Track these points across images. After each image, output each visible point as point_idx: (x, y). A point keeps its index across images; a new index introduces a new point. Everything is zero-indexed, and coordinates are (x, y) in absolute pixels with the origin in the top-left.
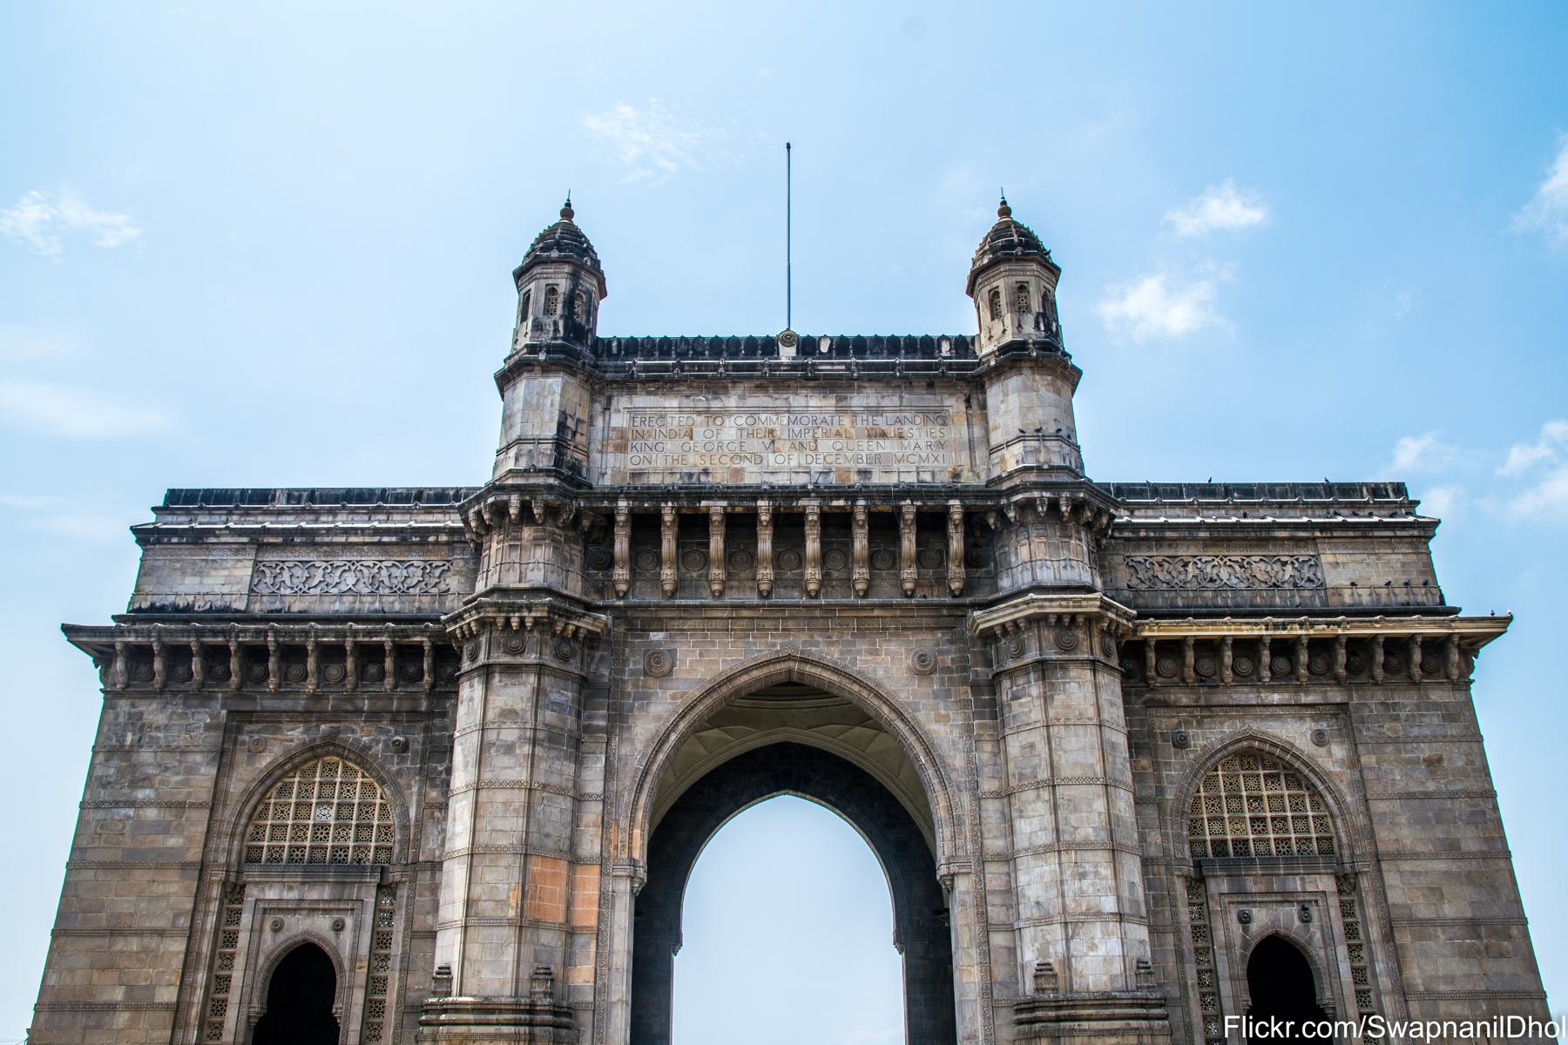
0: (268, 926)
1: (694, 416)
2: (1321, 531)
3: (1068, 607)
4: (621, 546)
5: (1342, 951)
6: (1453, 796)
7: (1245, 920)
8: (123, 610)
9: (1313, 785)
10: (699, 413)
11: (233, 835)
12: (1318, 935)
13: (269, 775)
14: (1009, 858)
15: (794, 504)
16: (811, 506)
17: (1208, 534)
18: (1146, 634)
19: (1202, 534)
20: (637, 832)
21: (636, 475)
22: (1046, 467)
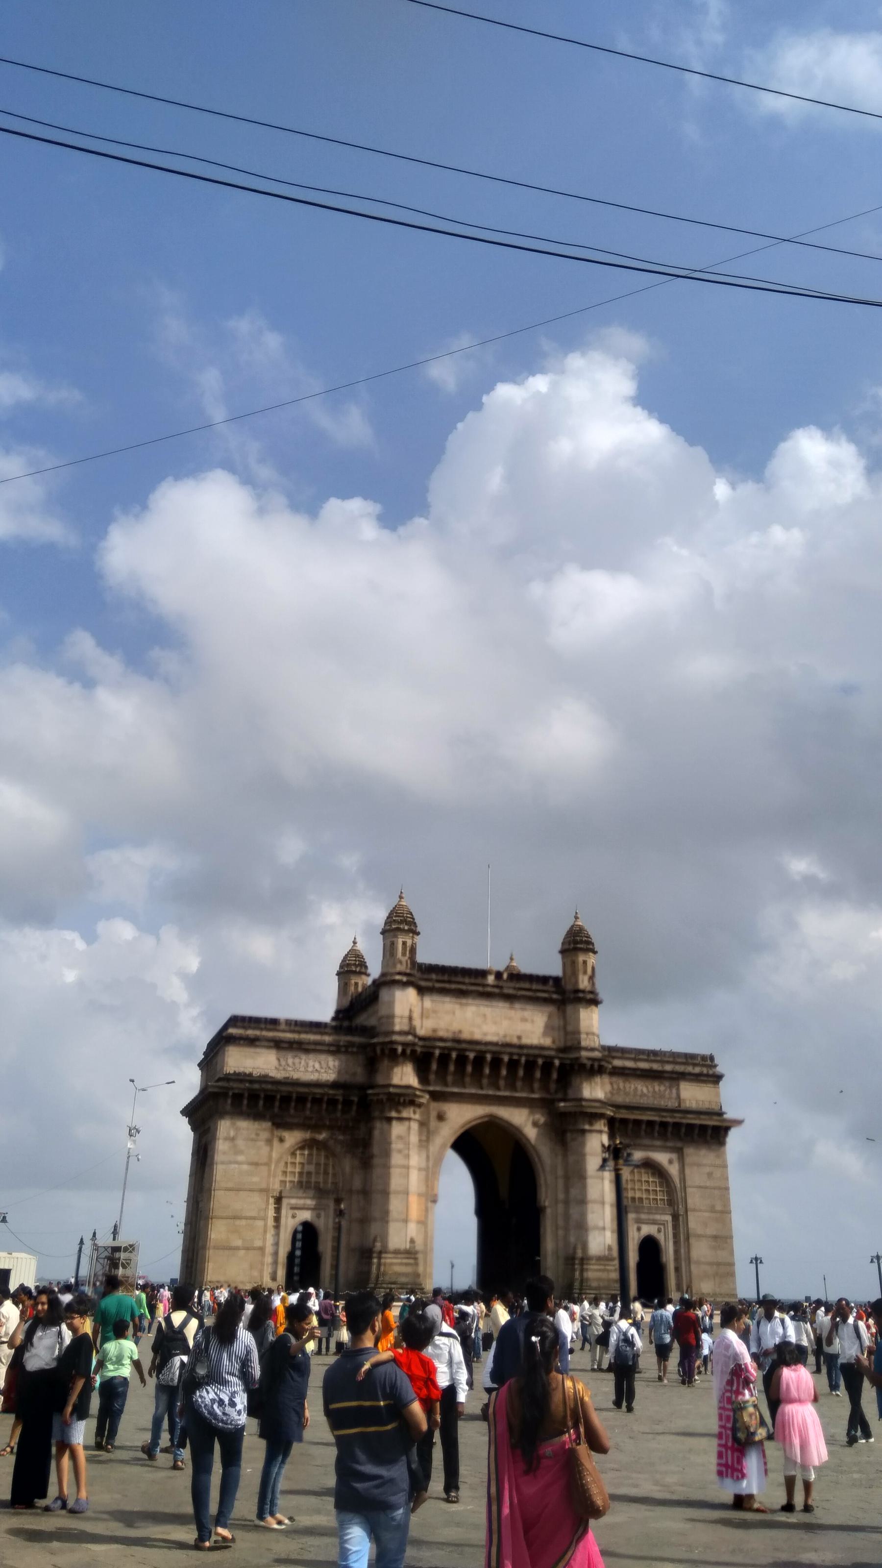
0: (290, 1215)
4: (434, 1066)
7: (639, 1229)
12: (663, 1237)
14: (567, 1202)
16: (506, 1058)
21: (435, 1031)
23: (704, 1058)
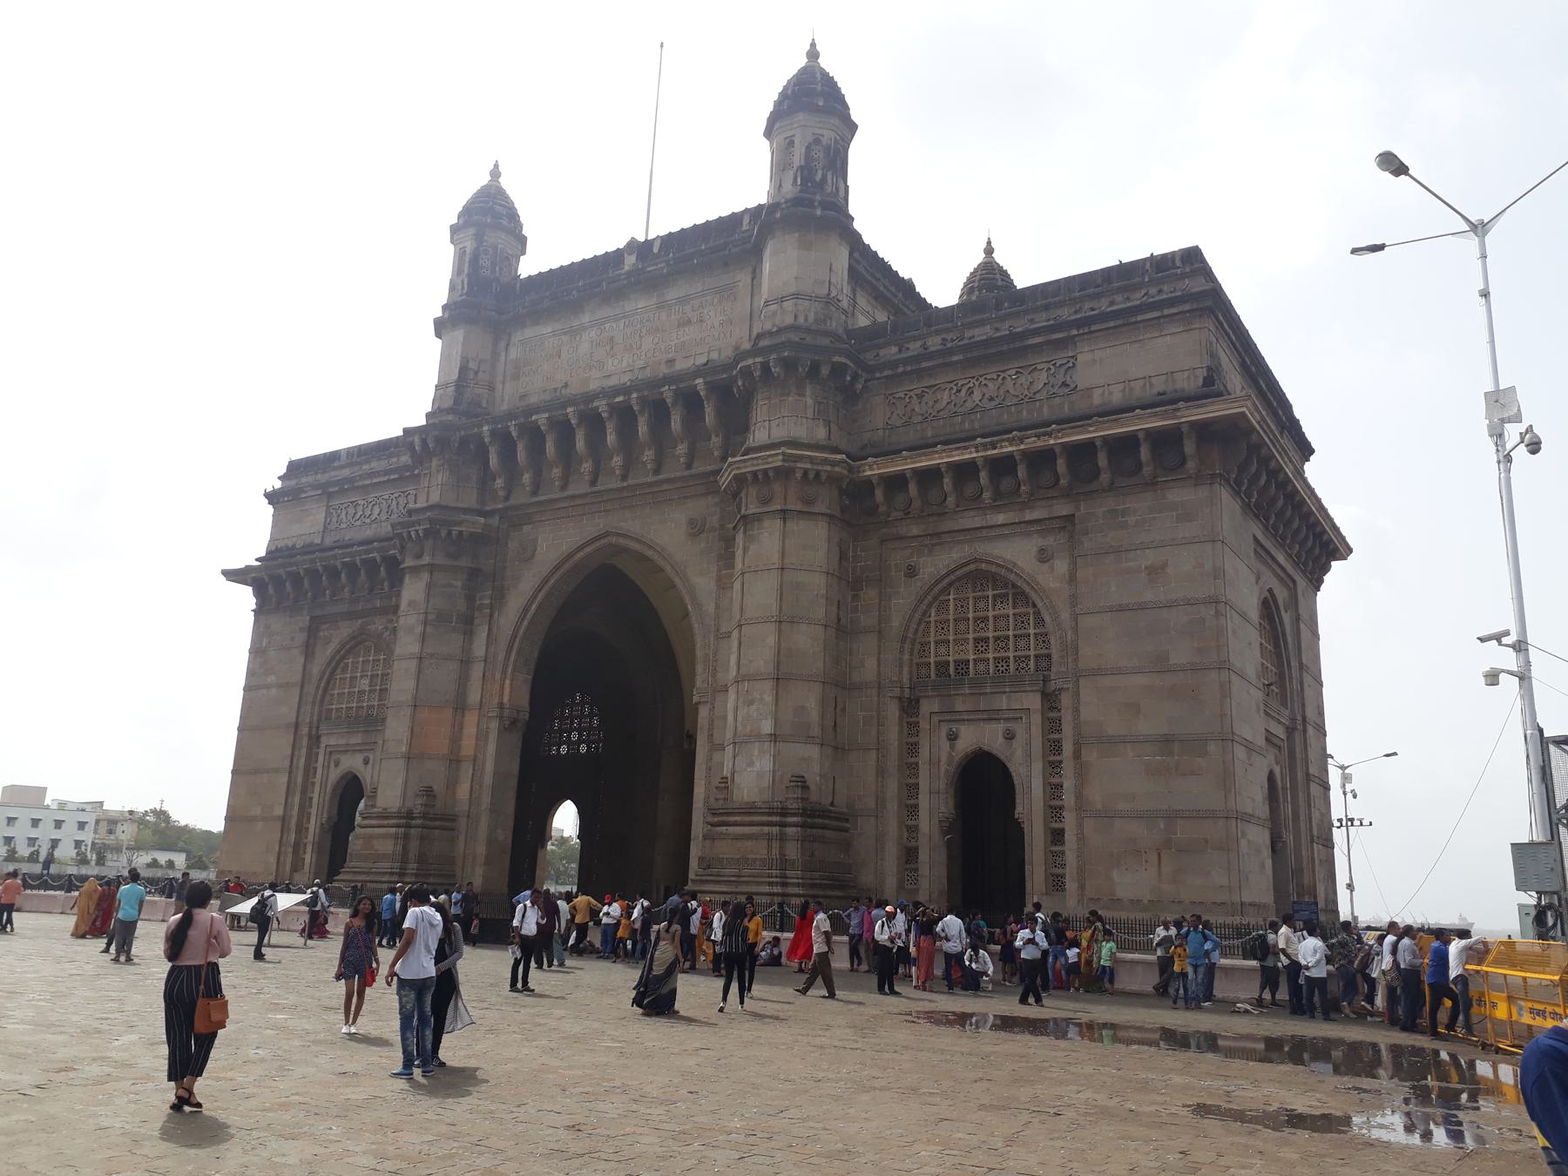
0: (332, 764)
1: (563, 337)
2: (1078, 329)
3: (758, 465)
4: (494, 461)
5: (1038, 767)
6: (1170, 605)
7: (953, 737)
8: (263, 553)
9: (1034, 605)
10: (565, 333)
11: (314, 702)
12: (1019, 752)
13: (333, 658)
15: (590, 406)
17: (960, 357)
18: (868, 473)
19: (955, 358)
20: (508, 682)
22: (775, 329)
23: (1161, 266)
